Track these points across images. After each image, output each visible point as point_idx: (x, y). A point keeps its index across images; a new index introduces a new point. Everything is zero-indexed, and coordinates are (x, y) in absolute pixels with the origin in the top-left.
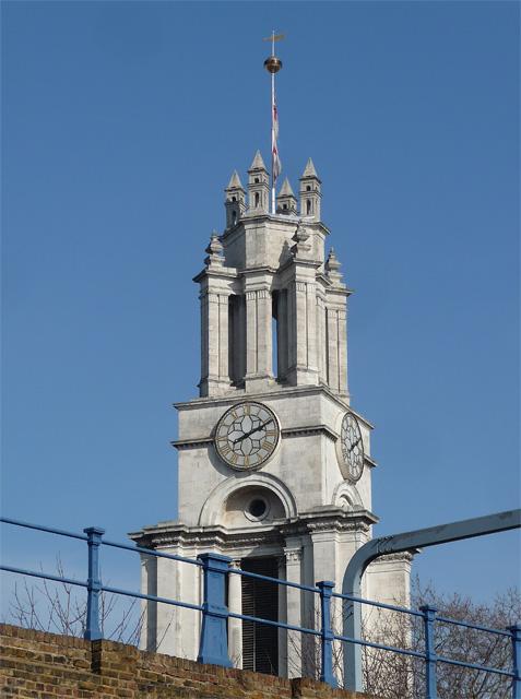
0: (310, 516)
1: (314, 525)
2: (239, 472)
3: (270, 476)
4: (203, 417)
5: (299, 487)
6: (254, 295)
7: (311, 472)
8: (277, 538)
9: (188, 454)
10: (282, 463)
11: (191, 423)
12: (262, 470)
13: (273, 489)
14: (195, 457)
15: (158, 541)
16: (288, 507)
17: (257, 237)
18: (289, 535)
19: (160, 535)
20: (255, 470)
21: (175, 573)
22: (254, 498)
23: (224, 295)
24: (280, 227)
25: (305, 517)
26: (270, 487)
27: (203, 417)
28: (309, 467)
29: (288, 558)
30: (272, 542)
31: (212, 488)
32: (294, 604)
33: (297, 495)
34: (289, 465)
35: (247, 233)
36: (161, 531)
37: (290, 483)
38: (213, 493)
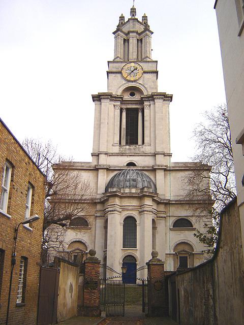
1: (156, 97)
2: (129, 81)
3: (140, 84)
7: (153, 84)
8: (141, 102)
11: (113, 67)
15: (103, 97)
16: (145, 93)
17: (133, 24)
18: (145, 100)
19: (103, 95)
20: (135, 81)
32: (147, 121)
34: (146, 82)
37: (146, 86)
38: (120, 87)
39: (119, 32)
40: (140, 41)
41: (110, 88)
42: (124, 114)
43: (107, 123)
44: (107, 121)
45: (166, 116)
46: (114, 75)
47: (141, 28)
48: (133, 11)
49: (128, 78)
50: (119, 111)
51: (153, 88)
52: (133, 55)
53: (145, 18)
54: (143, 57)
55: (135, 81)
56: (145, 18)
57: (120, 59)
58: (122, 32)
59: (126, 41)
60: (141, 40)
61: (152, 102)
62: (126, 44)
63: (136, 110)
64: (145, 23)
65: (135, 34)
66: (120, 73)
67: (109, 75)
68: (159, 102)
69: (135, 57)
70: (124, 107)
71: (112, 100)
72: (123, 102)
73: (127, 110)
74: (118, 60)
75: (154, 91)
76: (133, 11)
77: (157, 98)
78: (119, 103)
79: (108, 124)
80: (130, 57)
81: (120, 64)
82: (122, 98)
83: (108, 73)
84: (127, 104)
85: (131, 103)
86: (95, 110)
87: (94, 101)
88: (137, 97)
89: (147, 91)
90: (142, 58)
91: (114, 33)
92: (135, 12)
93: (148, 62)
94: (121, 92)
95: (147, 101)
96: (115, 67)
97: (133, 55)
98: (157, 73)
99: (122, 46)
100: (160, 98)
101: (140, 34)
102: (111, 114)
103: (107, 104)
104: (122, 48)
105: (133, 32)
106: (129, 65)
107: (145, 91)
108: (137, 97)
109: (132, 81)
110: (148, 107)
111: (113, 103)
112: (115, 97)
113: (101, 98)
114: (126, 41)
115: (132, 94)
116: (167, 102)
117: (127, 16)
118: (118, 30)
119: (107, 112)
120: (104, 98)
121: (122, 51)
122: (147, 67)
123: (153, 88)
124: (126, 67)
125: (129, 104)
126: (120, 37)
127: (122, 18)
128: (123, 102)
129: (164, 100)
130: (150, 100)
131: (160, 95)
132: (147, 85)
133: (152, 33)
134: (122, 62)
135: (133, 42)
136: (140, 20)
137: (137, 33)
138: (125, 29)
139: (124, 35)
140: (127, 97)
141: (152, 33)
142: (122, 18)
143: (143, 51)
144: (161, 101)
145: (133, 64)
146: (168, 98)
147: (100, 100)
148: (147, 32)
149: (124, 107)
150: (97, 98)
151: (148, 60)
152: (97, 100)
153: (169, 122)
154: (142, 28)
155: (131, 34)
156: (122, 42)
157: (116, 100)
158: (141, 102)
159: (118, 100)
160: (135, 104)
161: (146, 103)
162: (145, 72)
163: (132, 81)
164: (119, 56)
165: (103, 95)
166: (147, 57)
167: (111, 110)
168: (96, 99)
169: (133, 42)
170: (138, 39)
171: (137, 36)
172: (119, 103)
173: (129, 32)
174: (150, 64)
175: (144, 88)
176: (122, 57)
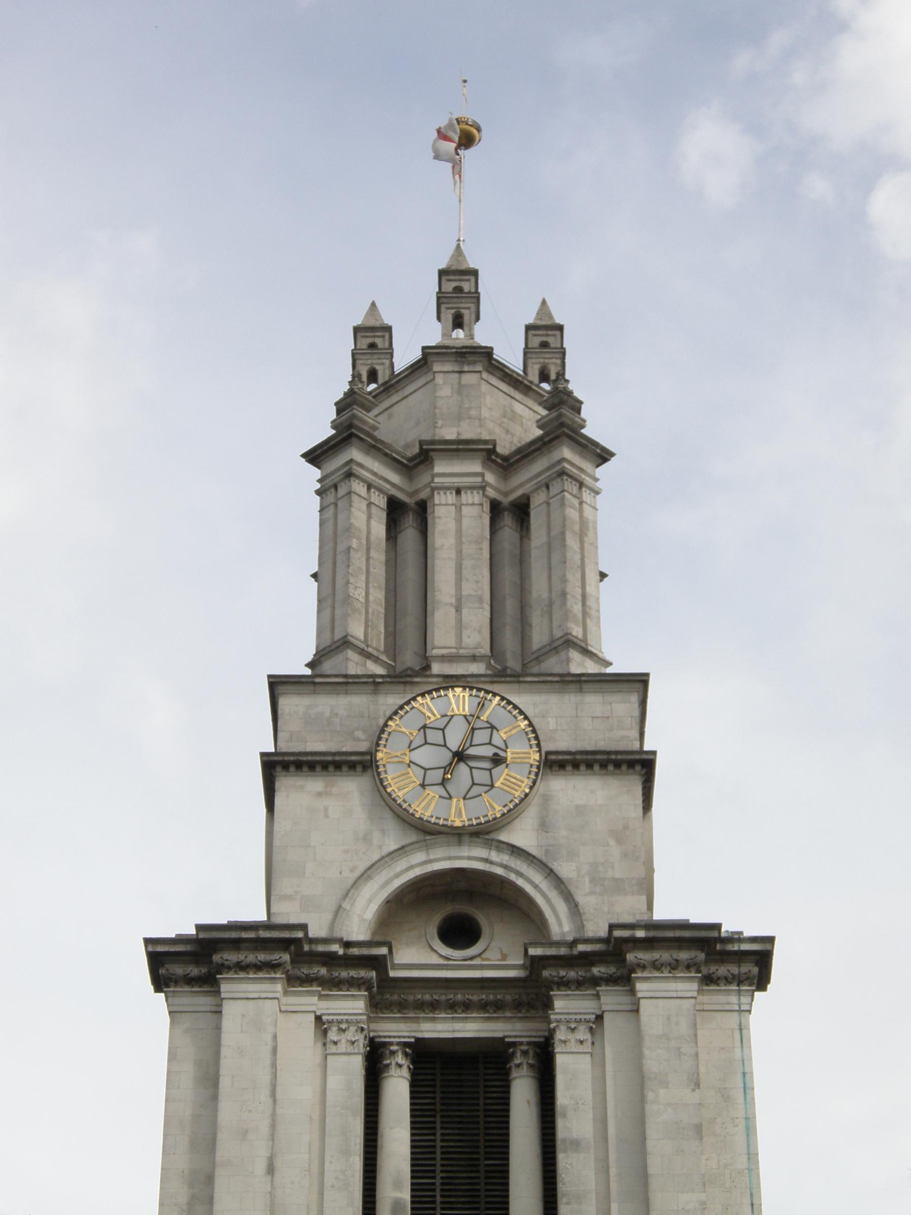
0: (640, 934)
3: (516, 851)
4: (342, 712)
5: (587, 885)
6: (451, 497)
7: (615, 851)
8: (530, 994)
9: (302, 787)
10: (544, 826)
12: (503, 837)
13: (520, 882)
14: (319, 794)
15: (232, 957)
16: (560, 925)
17: (460, 389)
18: (564, 984)
19: (236, 944)
21: (268, 1038)
22: (449, 909)
23: (380, 490)
24: (504, 386)
25: (625, 934)
26: (512, 877)
27: (342, 712)
28: (612, 842)
29: (560, 1035)
30: (498, 1006)
31: (362, 866)
32: (576, 1145)
33: (584, 899)
35: (439, 379)
36: (244, 935)
37: (565, 870)
39: (355, 454)
40: (512, 514)
41: (284, 886)
42: (397, 1090)
43: (261, 1167)
44: (262, 1151)
45: (727, 1099)
46: (314, 784)
47: (517, 421)
48: (458, 291)
49: (427, 806)
50: (356, 1064)
51: (618, 887)
52: (460, 621)
53: (545, 336)
54: (538, 638)
55: (481, 833)
56: (545, 336)
57: (366, 655)
58: (377, 448)
59: (407, 516)
60: (521, 511)
61: (611, 999)
62: (409, 535)
63: (492, 1059)
64: (544, 376)
65: (475, 466)
66: (362, 764)
67: (285, 784)
68: (666, 999)
69: (477, 637)
70: (397, 1030)
71: (307, 980)
72: (390, 994)
73: (423, 1055)
74: (354, 664)
75: (627, 909)
76: (458, 291)
77: (656, 966)
78: (353, 1005)
79: (271, 1170)
80: (442, 637)
81: (358, 701)
82: (378, 964)
83: (274, 767)
84: (420, 1006)
85: (452, 1006)
86: (172, 1057)
87: (160, 982)
88: (498, 955)
89: (575, 909)
90: (534, 648)
91: (314, 456)
92: (476, 297)
93: (581, 682)
94: (374, 907)
95: (580, 984)
96: (326, 723)
97: (460, 621)
98: (643, 766)
99: (379, 556)
100: (674, 966)
101: (507, 464)
102: (300, 1092)
103: (262, 1015)
104: (379, 570)
105: (461, 448)
106: (429, 707)
107: (562, 908)
108: (498, 955)
109: (458, 835)
110: (583, 1033)
111: (311, 1002)
112: (329, 959)
113: (223, 967)
114: (407, 516)
115: (459, 933)
116: (728, 997)
117: (415, 331)
118: (349, 430)
119: (267, 1079)
120: (241, 967)
121: (378, 595)
122: (571, 721)
123: (618, 887)
124: (404, 727)
125: (434, 1006)
126: (359, 487)
127: (372, 338)
128: (390, 994)
129: (709, 980)
130: (595, 982)
131: (681, 943)
132: (571, 859)
133: (603, 456)
134: (373, 684)
135: (459, 525)
136: (511, 355)
137: (487, 452)
138: (399, 424)
139: (395, 478)
140: (418, 955)
141: (603, 456)
142: (372, 338)
143: (539, 587)
144: (688, 987)
145: (460, 701)
146: (734, 963)
147: (209, 982)
148: (567, 452)
149: (397, 1030)
150: (191, 965)
151: (579, 665)
152: (189, 981)
153: (752, 1156)
154: (522, 421)
155: (440, 467)
156: (379, 529)
157: (336, 984)
158: (530, 994)
159: (352, 983)
160: (483, 1006)
161: (564, 1004)
162: (557, 763)
163: (458, 835)
164: (357, 630)
165: (236, 944)
166: (569, 642)
167: (298, 1059)
168: (178, 970)
169: (459, 525)
170: (496, 509)
171: (490, 478)
172: (353, 1005)
173: (425, 455)
174: (594, 702)
175: (544, 885)
176: (378, 642)
